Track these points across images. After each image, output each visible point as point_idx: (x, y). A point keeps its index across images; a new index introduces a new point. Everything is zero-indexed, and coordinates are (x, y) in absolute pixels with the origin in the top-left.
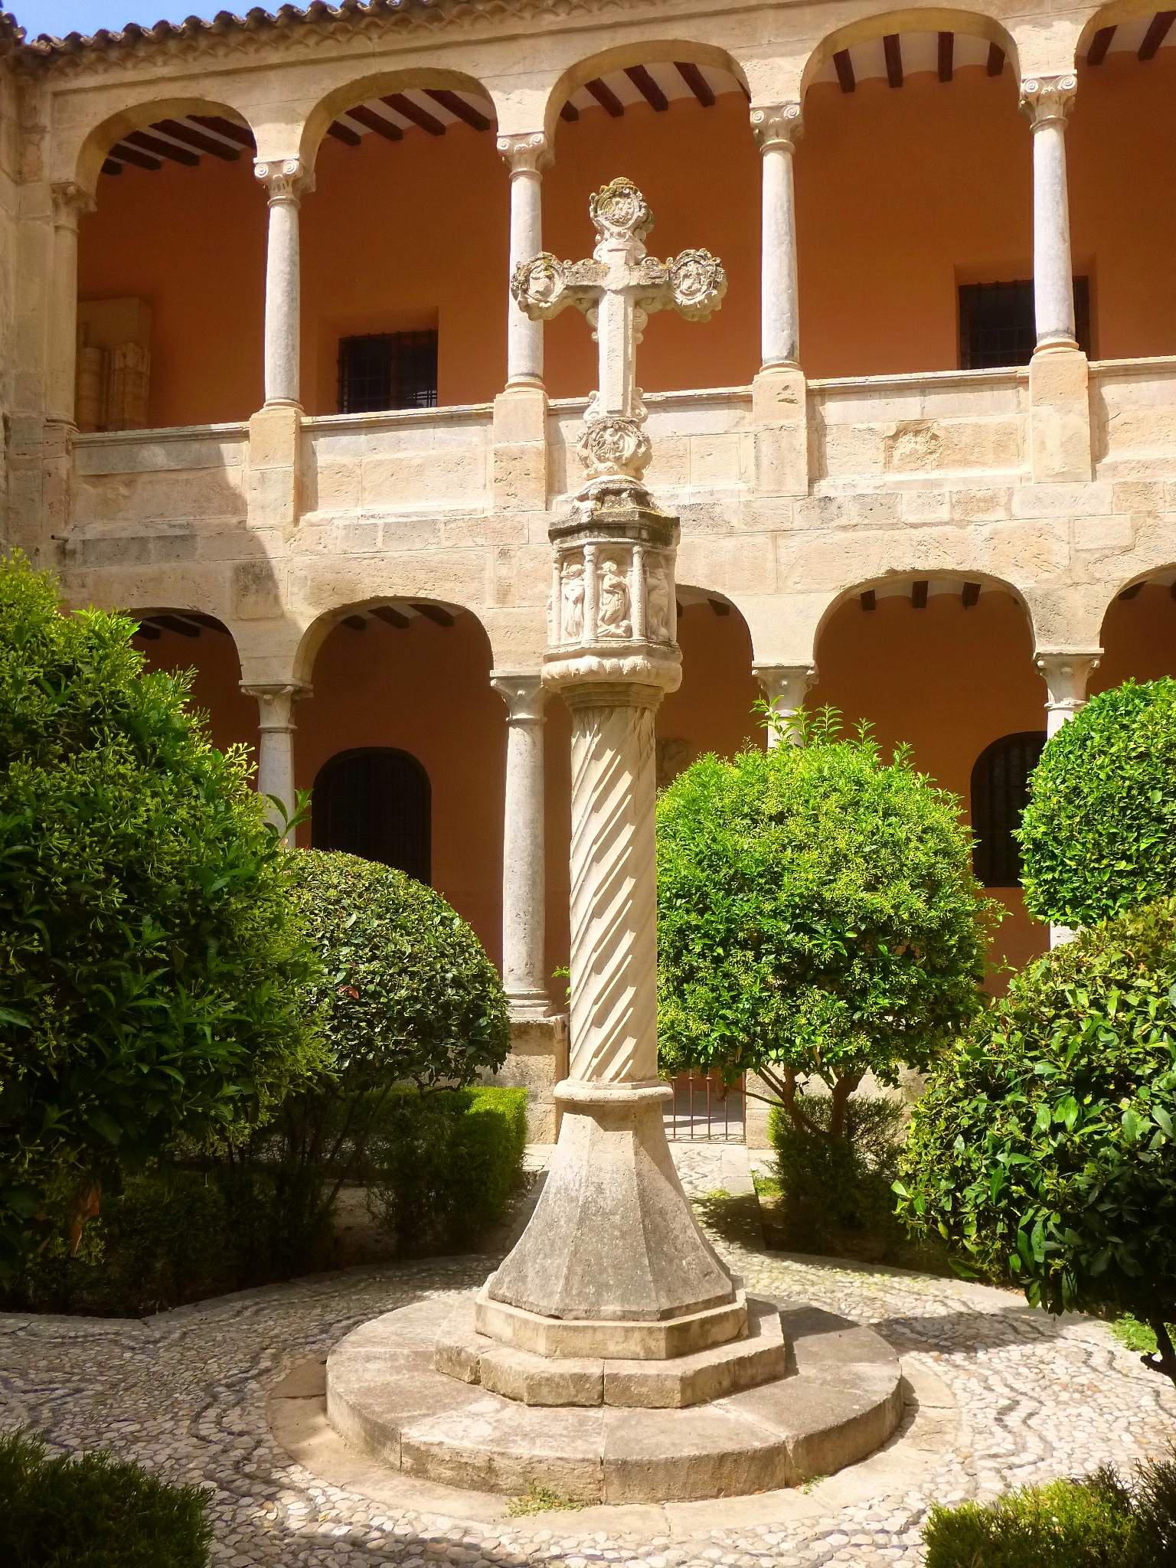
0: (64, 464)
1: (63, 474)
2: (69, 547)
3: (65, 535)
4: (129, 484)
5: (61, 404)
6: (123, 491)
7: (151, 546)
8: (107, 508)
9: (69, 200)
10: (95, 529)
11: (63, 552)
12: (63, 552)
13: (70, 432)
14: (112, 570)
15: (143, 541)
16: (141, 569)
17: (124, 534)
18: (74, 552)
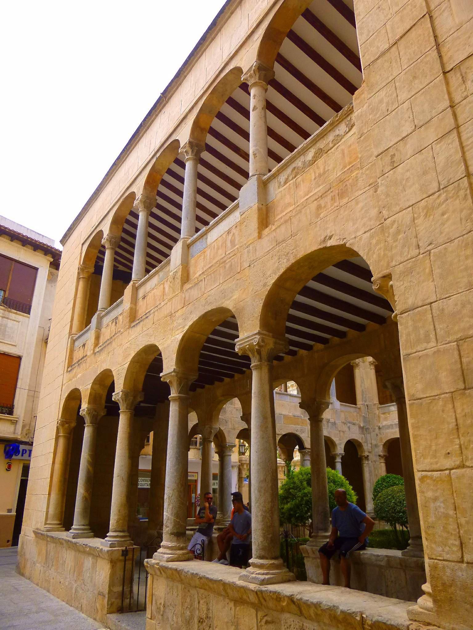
0: (377, 412)
1: (377, 414)
2: (380, 427)
3: (379, 425)
4: (389, 414)
5: (376, 401)
6: (388, 415)
7: (394, 426)
8: (386, 419)
9: (372, 364)
10: (385, 423)
11: (379, 428)
12: (379, 428)
13: (378, 405)
14: (388, 431)
15: (392, 425)
16: (393, 430)
17: (389, 424)
18: (381, 428)
